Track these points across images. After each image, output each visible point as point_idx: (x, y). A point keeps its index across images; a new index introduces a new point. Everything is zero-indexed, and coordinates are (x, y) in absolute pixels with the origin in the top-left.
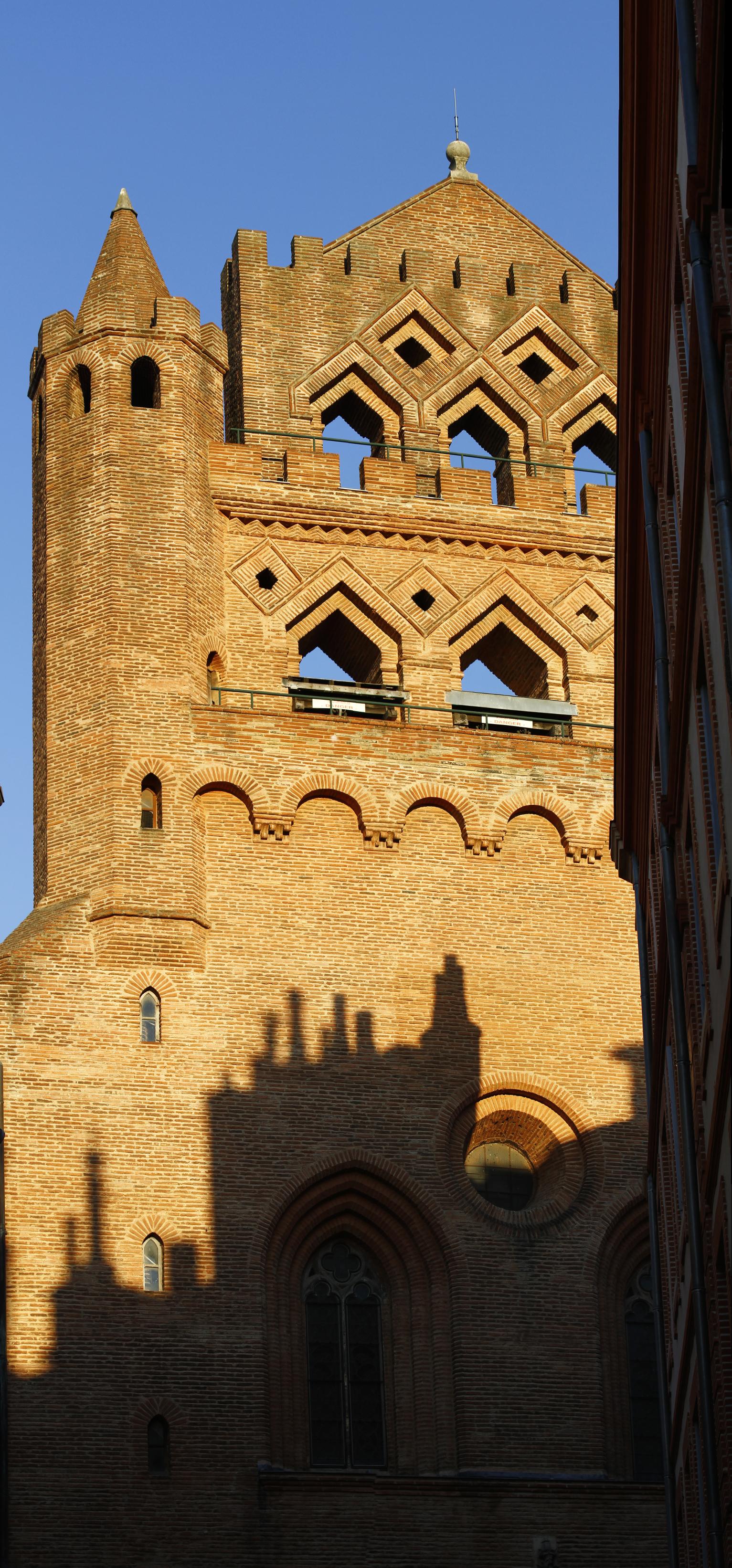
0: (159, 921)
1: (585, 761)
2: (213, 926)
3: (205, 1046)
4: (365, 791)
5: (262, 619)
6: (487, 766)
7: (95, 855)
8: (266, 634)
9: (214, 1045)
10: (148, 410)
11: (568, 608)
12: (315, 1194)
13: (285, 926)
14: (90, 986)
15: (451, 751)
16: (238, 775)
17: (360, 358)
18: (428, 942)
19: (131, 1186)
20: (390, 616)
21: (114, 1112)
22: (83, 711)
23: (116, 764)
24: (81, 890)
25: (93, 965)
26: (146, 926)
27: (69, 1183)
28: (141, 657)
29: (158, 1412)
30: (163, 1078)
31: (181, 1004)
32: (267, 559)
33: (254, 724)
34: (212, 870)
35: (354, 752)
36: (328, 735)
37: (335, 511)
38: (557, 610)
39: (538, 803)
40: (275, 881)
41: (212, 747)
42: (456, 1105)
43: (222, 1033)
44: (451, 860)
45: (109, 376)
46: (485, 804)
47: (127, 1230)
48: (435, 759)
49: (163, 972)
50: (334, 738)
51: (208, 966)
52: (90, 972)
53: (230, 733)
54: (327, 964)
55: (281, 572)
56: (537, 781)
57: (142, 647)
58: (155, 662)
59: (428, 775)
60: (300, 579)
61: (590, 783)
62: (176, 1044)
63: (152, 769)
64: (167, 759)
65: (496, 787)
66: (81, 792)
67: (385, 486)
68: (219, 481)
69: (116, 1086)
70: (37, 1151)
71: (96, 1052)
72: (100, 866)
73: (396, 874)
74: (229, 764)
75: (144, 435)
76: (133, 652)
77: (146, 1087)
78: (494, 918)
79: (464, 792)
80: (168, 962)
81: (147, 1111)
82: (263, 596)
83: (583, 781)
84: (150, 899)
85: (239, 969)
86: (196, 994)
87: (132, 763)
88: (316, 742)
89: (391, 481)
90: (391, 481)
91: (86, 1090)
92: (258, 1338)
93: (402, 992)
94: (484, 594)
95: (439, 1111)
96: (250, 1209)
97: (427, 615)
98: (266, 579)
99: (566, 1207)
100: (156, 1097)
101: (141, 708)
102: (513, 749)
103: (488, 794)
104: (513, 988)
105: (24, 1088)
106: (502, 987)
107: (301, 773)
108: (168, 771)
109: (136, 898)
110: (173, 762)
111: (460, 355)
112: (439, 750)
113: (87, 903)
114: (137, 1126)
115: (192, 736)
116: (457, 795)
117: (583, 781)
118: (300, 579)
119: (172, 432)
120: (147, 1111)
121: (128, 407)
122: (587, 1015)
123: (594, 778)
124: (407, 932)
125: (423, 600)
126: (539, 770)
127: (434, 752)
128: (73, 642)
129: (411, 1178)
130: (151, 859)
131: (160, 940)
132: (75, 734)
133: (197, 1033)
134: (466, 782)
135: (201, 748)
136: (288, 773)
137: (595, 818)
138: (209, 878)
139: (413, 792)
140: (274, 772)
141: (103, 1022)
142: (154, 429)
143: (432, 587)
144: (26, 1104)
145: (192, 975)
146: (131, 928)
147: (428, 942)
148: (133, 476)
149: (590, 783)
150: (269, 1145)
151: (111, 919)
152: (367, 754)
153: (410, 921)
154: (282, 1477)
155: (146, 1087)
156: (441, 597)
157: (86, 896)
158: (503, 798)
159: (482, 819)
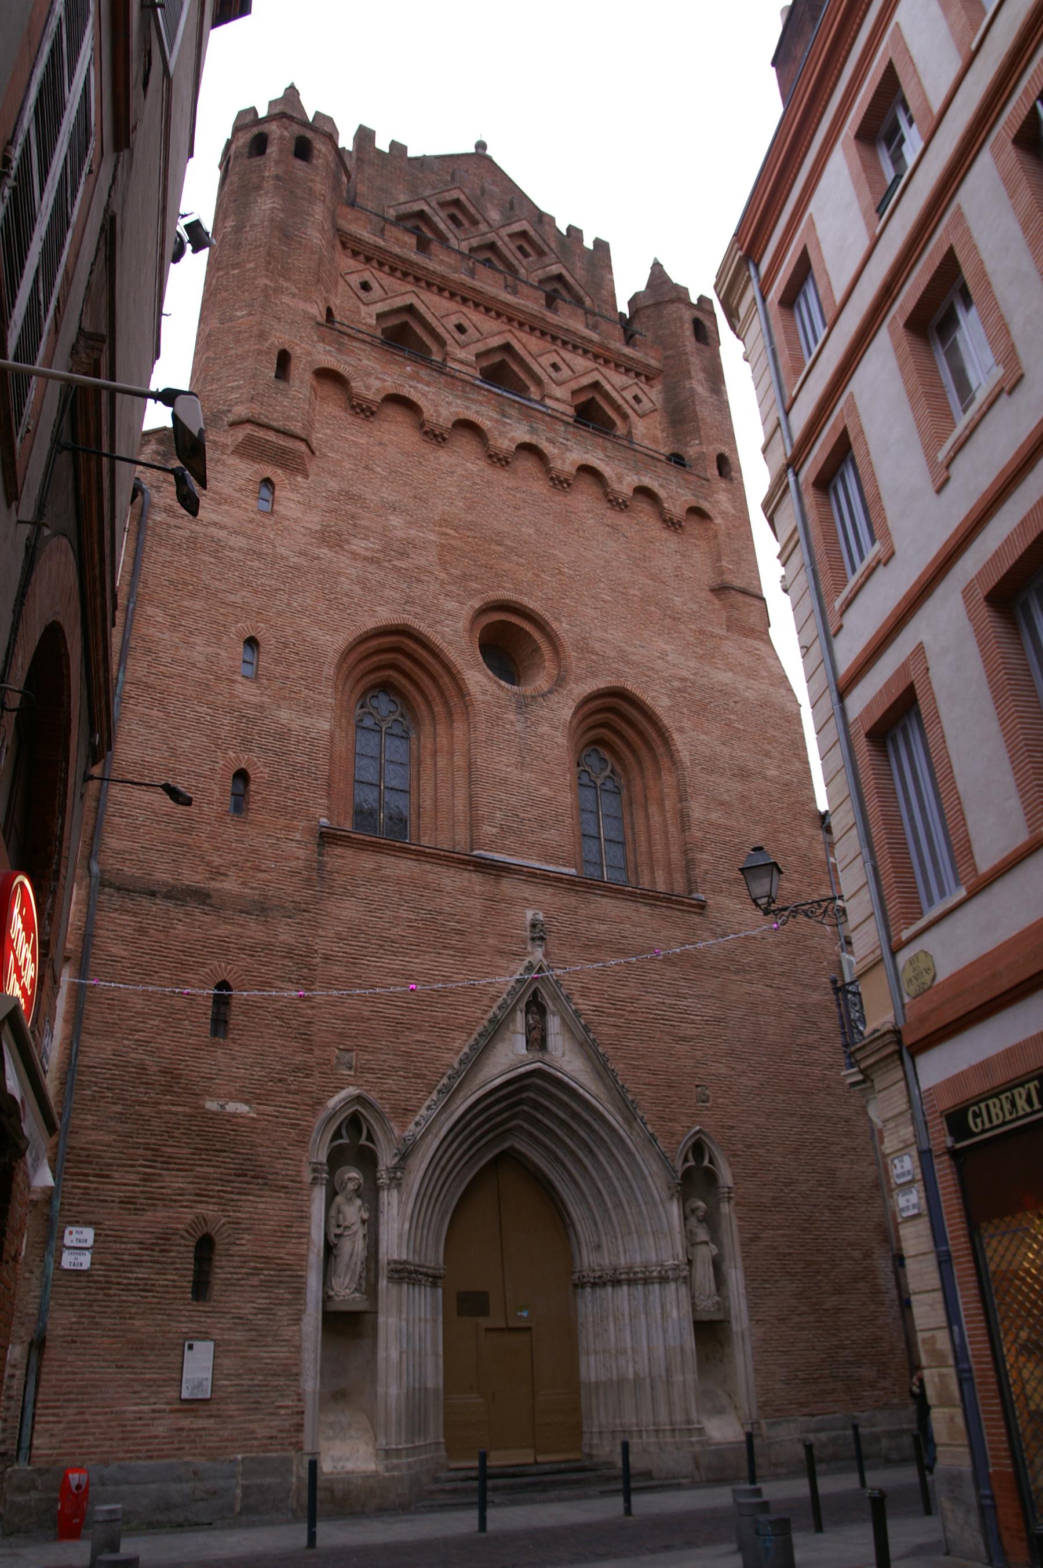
0: (281, 435)
1: (562, 429)
2: (317, 453)
3: (305, 525)
4: (427, 404)
5: (362, 306)
6: (504, 414)
7: (239, 387)
8: (363, 314)
9: (309, 526)
10: (304, 163)
11: (546, 360)
12: (374, 643)
13: (366, 467)
14: (224, 464)
15: (481, 398)
16: (343, 369)
17: (426, 208)
18: (460, 504)
19: (239, 600)
20: (440, 330)
21: (230, 547)
22: (240, 309)
23: (262, 336)
24: (226, 408)
25: (229, 452)
26: (271, 436)
27: (191, 587)
28: (286, 284)
29: (243, 766)
30: (272, 536)
31: (290, 495)
32: (367, 276)
33: (357, 344)
34: (319, 421)
35: (420, 380)
36: (406, 365)
37: (412, 263)
38: (539, 359)
39: (534, 442)
40: (363, 441)
41: (328, 348)
42: (477, 606)
43: (317, 519)
44: (477, 462)
45: (282, 137)
46: (501, 433)
47: (233, 630)
48: (472, 400)
49: (280, 472)
50: (408, 368)
51: (311, 477)
52: (225, 457)
53: (342, 344)
54: (394, 498)
55: (375, 285)
56: (533, 431)
57: (288, 279)
58: (294, 289)
59: (468, 408)
60: (386, 293)
61: (565, 442)
62: (286, 518)
63: (286, 347)
64: (297, 345)
65: (509, 427)
66: (233, 352)
67: (442, 260)
68: (342, 223)
69: (235, 532)
70: (168, 559)
71: (225, 507)
72: (242, 394)
73: (442, 460)
74: (339, 361)
75: (301, 174)
76: (281, 280)
77: (259, 539)
78: (504, 502)
79: (488, 422)
80: (283, 466)
81: (259, 555)
82: (362, 294)
83: (561, 440)
84: (275, 420)
85: (333, 485)
86: (301, 491)
87: (272, 339)
88: (396, 367)
89: (446, 259)
90: (446, 259)
91: (212, 530)
92: (327, 727)
93: (443, 529)
94: (496, 338)
95: (465, 607)
96: (328, 637)
97: (463, 337)
98: (365, 286)
99: (546, 690)
100: (266, 548)
101: (283, 312)
102: (519, 410)
103: (504, 429)
104: (514, 545)
105: (164, 515)
106: (508, 542)
107: (386, 381)
108: (296, 351)
109: (267, 417)
110: (302, 348)
111: (483, 227)
112: (475, 397)
113: (229, 415)
114: (249, 563)
115: (315, 338)
116: (486, 424)
117: (561, 440)
118: (386, 293)
119: (318, 179)
120: (259, 555)
121: (291, 156)
122: (561, 573)
123: (567, 440)
124: (447, 495)
125: (461, 329)
126: (535, 425)
127: (470, 396)
128: (237, 271)
129: (445, 645)
130: (279, 397)
131: (280, 447)
132: (231, 320)
133: (299, 515)
134: (491, 419)
135: (320, 346)
136: (377, 378)
137: (568, 461)
138: (317, 425)
139: (457, 413)
140: (369, 375)
141: (231, 490)
142: (307, 173)
143: (466, 324)
144: (165, 526)
145: (299, 479)
146: (261, 433)
147: (460, 504)
148: (292, 192)
149: (565, 442)
150: (345, 599)
151: (247, 425)
152: (428, 384)
153: (450, 489)
154: (339, 833)
155: (259, 539)
156: (471, 330)
157: (229, 411)
158: (513, 434)
159: (500, 441)
